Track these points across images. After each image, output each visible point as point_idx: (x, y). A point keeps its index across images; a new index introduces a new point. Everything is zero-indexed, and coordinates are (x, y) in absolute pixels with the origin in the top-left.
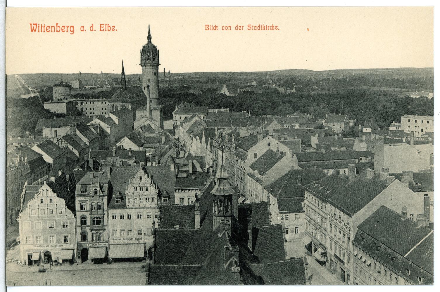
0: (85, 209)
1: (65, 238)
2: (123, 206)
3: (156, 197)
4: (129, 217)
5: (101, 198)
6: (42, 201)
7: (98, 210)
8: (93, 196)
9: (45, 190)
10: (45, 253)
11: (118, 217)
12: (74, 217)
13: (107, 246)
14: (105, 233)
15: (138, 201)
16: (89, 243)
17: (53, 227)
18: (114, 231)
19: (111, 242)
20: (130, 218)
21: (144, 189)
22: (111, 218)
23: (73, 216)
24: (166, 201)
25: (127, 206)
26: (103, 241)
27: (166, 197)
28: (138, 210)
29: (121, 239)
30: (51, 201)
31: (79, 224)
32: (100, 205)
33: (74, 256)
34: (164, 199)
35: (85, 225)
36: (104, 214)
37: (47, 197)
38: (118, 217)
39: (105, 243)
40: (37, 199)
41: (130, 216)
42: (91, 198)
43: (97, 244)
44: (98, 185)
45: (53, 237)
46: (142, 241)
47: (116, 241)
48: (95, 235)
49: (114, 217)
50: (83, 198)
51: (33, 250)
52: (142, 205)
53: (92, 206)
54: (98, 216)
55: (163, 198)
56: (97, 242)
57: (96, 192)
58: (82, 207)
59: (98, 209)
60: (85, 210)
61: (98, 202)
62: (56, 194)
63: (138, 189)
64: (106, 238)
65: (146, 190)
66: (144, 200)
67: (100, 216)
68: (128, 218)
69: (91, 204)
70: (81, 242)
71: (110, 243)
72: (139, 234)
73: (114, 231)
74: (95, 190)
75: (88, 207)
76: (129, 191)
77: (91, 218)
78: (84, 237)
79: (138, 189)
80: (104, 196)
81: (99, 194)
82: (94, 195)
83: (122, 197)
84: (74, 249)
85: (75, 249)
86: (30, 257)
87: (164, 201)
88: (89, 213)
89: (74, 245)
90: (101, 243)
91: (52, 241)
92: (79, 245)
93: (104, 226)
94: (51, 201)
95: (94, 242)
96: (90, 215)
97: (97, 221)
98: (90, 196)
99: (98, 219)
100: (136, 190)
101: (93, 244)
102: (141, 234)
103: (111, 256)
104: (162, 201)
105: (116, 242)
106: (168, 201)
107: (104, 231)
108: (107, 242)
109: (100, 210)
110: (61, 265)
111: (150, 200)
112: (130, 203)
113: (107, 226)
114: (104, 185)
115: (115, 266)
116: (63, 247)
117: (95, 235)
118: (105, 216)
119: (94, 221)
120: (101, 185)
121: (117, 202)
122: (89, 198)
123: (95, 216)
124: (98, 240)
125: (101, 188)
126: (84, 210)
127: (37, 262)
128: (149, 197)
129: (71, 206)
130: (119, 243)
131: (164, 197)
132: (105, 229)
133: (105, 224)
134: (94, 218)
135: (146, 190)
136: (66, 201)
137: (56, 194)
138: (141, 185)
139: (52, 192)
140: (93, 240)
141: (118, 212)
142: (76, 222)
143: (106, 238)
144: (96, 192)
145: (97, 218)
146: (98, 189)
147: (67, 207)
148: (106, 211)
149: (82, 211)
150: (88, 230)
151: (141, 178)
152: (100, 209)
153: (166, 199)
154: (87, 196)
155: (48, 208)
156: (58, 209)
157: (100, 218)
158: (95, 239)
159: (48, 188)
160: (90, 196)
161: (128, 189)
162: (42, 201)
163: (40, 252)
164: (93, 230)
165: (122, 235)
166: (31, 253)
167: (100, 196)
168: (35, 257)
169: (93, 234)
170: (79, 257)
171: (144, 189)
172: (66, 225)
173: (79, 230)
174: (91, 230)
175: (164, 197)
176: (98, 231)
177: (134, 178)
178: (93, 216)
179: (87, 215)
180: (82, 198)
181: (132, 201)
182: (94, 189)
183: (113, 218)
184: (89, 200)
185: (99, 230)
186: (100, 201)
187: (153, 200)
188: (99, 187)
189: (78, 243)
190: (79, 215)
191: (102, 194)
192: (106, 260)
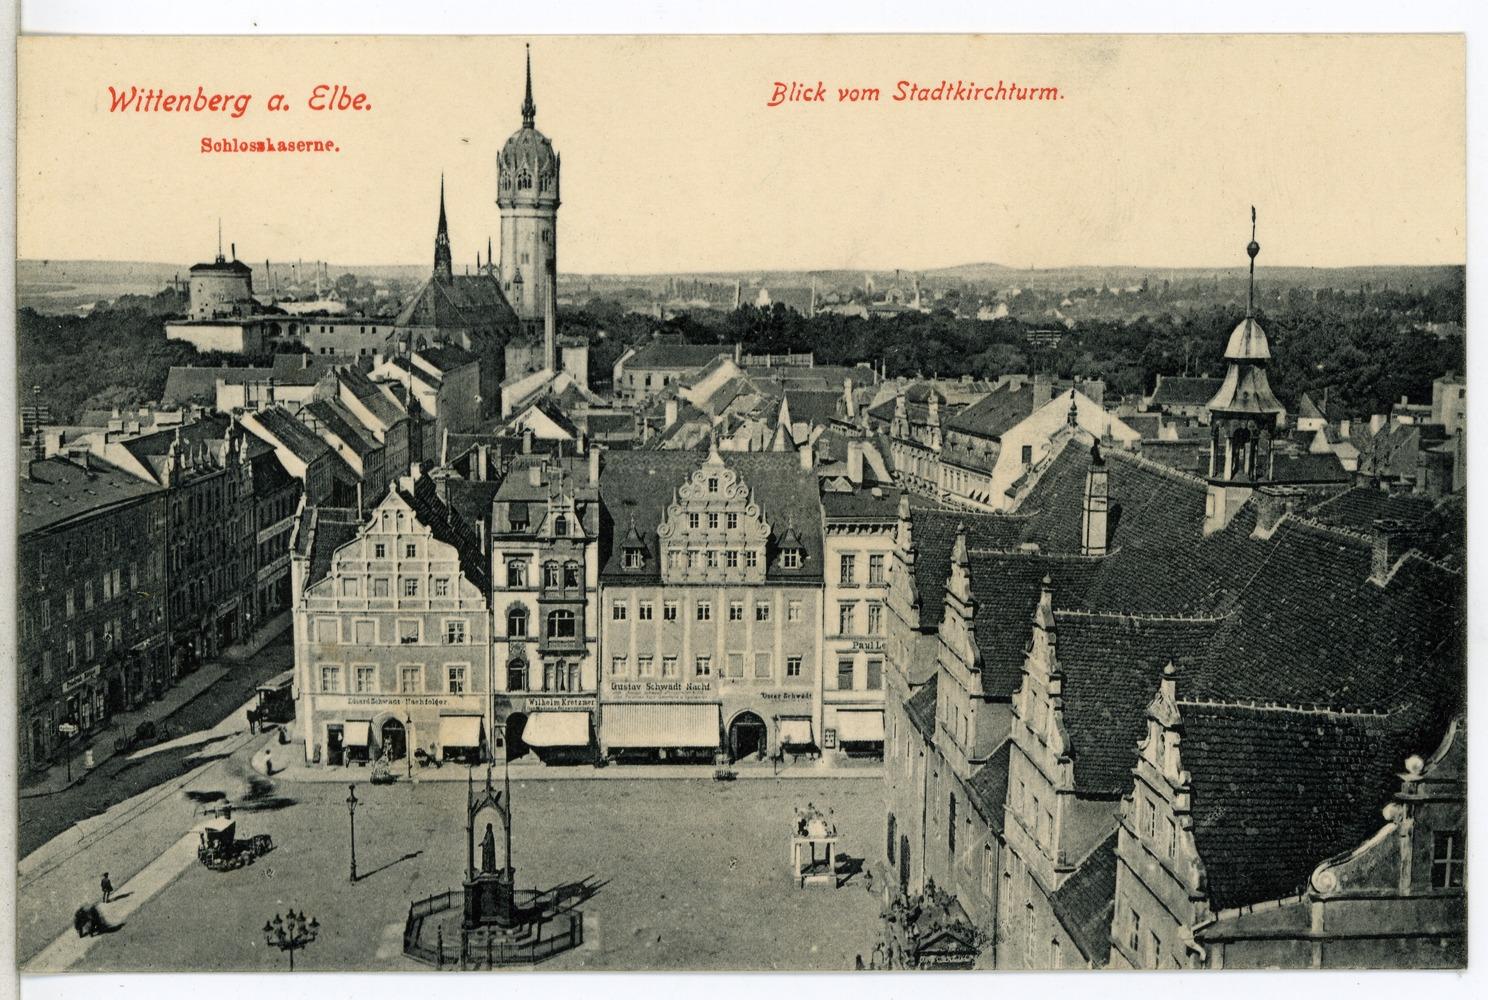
0: (521, 583)
1: (452, 676)
2: (654, 579)
3: (761, 550)
4: (670, 614)
5: (580, 545)
6: (380, 551)
7: (568, 588)
8: (553, 541)
9: (393, 516)
10: (385, 726)
11: (633, 613)
12: (488, 607)
13: (594, 707)
14: (588, 667)
15: (700, 561)
16: (535, 696)
17: (415, 640)
18: (618, 658)
19: (607, 693)
20: (674, 617)
21: (722, 520)
22: (608, 612)
23: (484, 604)
24: (793, 564)
25: (664, 578)
26: (581, 689)
27: (794, 552)
28: (700, 592)
29: (639, 687)
30: (411, 551)
31: (501, 628)
32: (572, 571)
33: (482, 736)
34: (787, 558)
35: (524, 638)
36: (585, 603)
37: (399, 537)
38: (633, 613)
39: (587, 699)
40: (364, 540)
41: (674, 610)
42: (546, 545)
43: (560, 700)
44: (570, 502)
45: (416, 674)
46: (709, 697)
47: (624, 692)
48: (552, 672)
49: (619, 613)
50: (519, 544)
51: (344, 712)
52: (713, 577)
53: (547, 572)
54: (565, 607)
55: (782, 556)
56: (560, 693)
57: (561, 525)
58: (513, 576)
59: (566, 585)
60: (524, 586)
61: (567, 558)
62: (428, 528)
63: (703, 519)
64: (589, 684)
65: (730, 526)
66: (721, 560)
67: (573, 608)
68: (666, 616)
69: (546, 568)
70: (506, 693)
71: (603, 699)
72: (699, 671)
73: (618, 658)
74: (559, 518)
75: (534, 574)
76: (675, 527)
77: (541, 613)
78: (517, 679)
79: (703, 519)
80: (587, 541)
81: (572, 534)
82: (554, 536)
83: (650, 549)
84: (482, 716)
85: (487, 715)
86: (335, 734)
87: (787, 564)
88: (536, 595)
89: (483, 701)
90: (573, 696)
91: (409, 687)
92: (500, 701)
93: (585, 641)
94: (411, 551)
95: (547, 693)
96: (540, 601)
97: (563, 624)
98: (542, 540)
99: (566, 618)
100: (694, 523)
101: (546, 700)
102: (707, 672)
103: (609, 739)
104: (782, 564)
105: (624, 696)
106: (801, 565)
107: (584, 658)
108: (594, 695)
109: (574, 588)
110: (439, 765)
111: (740, 559)
112: (672, 566)
113: (593, 641)
114: (589, 505)
115: (613, 771)
116: (443, 706)
117: (552, 672)
118: (587, 609)
119: (551, 624)
120: (580, 505)
121: (629, 563)
122: (537, 544)
123: (558, 607)
124: (563, 688)
125: (580, 514)
126: (518, 587)
127: (360, 754)
128: (739, 549)
129: (476, 570)
130: (633, 700)
131: (787, 552)
132: (586, 653)
133: (591, 633)
134: (552, 614)
135: (730, 526)
136: (460, 553)
137: (428, 528)
138: (712, 509)
139: (416, 523)
140: (545, 688)
141: (632, 597)
142: (492, 625)
143: (589, 684)
144: (561, 525)
145: (562, 613)
146: (571, 517)
147: (463, 573)
148: (594, 590)
149: (512, 587)
150: (531, 651)
151: (713, 483)
152: (574, 584)
153: (794, 558)
154: (532, 539)
155: (400, 577)
156: (433, 580)
157: (571, 614)
158: (552, 683)
159: (404, 506)
160: (542, 540)
161: (669, 521)
162: (380, 551)
163: (371, 722)
164: (550, 653)
165: (645, 674)
166: (341, 722)
167: (575, 541)
168: (355, 736)
169: (547, 666)
170: (499, 743)
171: (722, 520)
172: (457, 633)
173: (502, 652)
174: (543, 653)
175: (787, 552)
176: (565, 659)
177: (690, 480)
178: (551, 608)
179: (530, 601)
180: (516, 547)
181: (680, 560)
182: (556, 515)
183: (616, 617)
184: (536, 553)
185: (567, 653)
186: (576, 558)
187: (752, 559)
188: (572, 509)
189: (497, 696)
190: (503, 601)
191: (580, 535)
192: (586, 754)
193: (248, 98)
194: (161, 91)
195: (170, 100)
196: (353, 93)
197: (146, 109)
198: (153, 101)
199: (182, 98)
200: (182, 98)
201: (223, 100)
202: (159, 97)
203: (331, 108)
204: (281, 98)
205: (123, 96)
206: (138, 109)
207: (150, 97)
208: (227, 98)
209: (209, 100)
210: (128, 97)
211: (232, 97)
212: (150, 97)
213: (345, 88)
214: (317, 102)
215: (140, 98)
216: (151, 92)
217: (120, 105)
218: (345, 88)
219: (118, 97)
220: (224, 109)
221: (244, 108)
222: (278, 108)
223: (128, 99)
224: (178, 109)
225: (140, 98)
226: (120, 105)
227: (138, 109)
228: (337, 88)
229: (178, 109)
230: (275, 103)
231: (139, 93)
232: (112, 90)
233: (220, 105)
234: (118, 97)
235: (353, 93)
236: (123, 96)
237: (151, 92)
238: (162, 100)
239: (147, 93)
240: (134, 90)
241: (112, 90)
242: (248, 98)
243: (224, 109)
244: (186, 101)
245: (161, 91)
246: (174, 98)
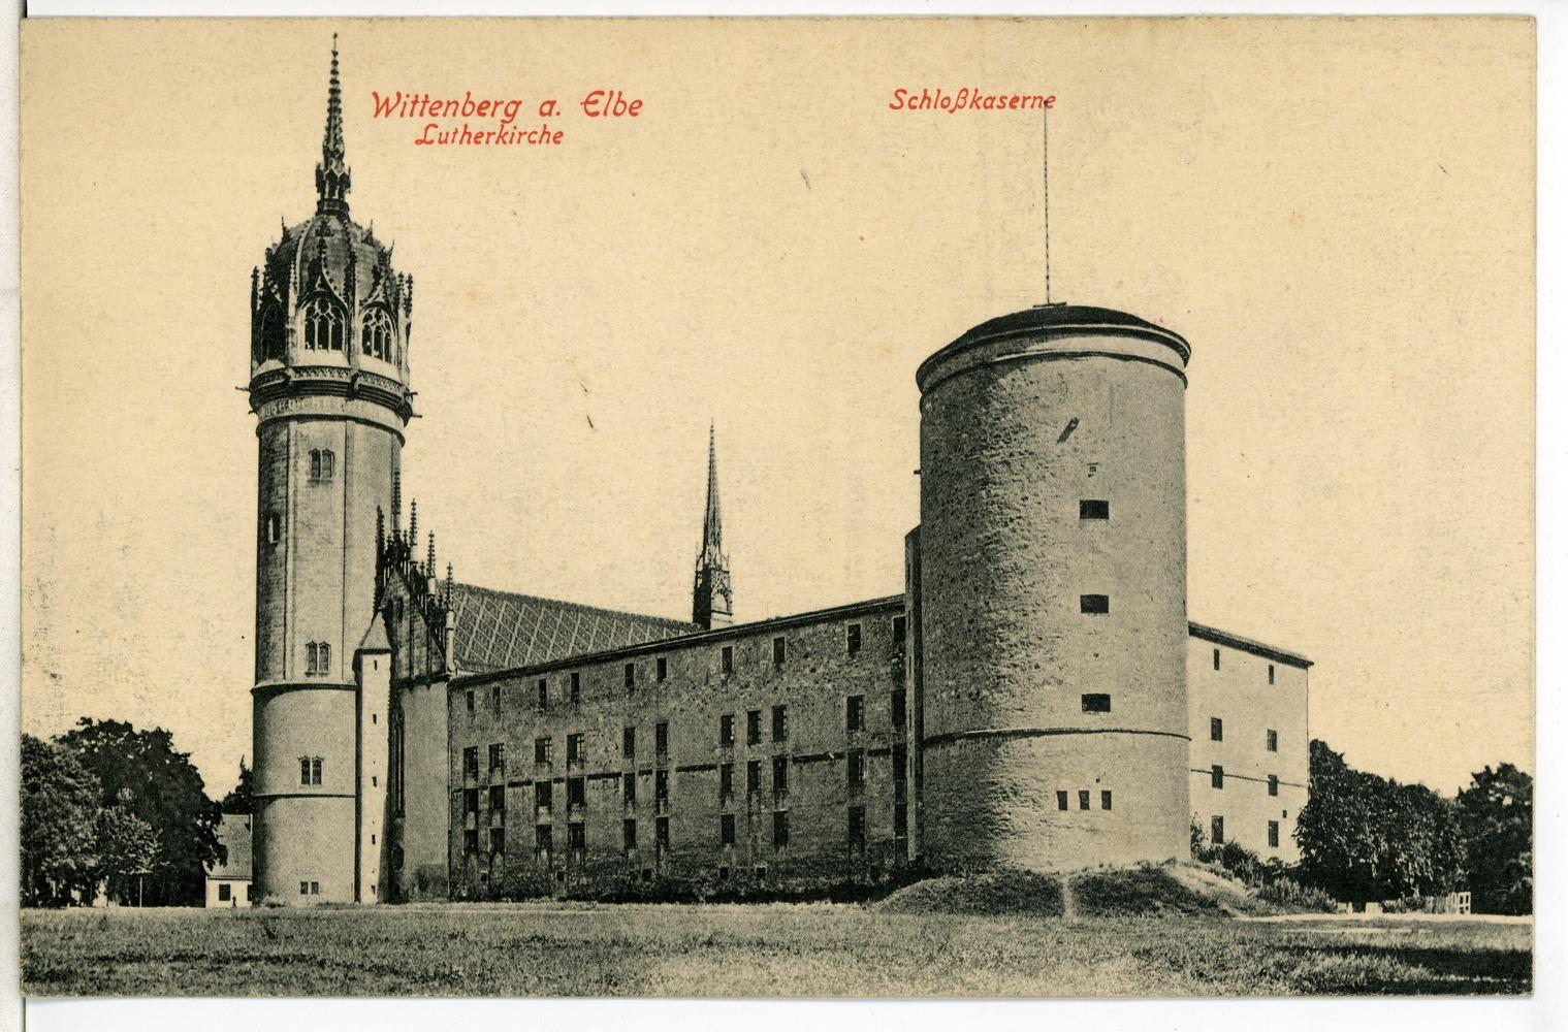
193: (518, 104)
194: (427, 96)
195: (437, 105)
196: (628, 98)
197: (411, 115)
198: (419, 107)
199: (449, 104)
200: (449, 104)
201: (492, 105)
202: (426, 102)
203: (605, 113)
204: (552, 103)
205: (387, 101)
206: (402, 115)
207: (415, 103)
208: (497, 104)
209: (477, 105)
210: (392, 103)
211: (502, 102)
212: (415, 103)
213: (620, 94)
214: (592, 109)
215: (405, 103)
216: (417, 96)
217: (384, 111)
218: (620, 94)
219: (382, 100)
220: (493, 114)
221: (514, 115)
222: (550, 114)
223: (391, 104)
224: (445, 115)
225: (405, 103)
226: (384, 111)
227: (402, 115)
228: (612, 93)
229: (445, 115)
230: (546, 108)
231: (403, 99)
232: (375, 95)
233: (489, 111)
234: (381, 105)
235: (628, 98)
236: (387, 101)
237: (417, 96)
238: (428, 106)
239: (412, 98)
240: (399, 95)
241: (375, 95)
242: (518, 104)
243: (493, 114)
244: (453, 106)
245: (427, 96)
246: (440, 103)
